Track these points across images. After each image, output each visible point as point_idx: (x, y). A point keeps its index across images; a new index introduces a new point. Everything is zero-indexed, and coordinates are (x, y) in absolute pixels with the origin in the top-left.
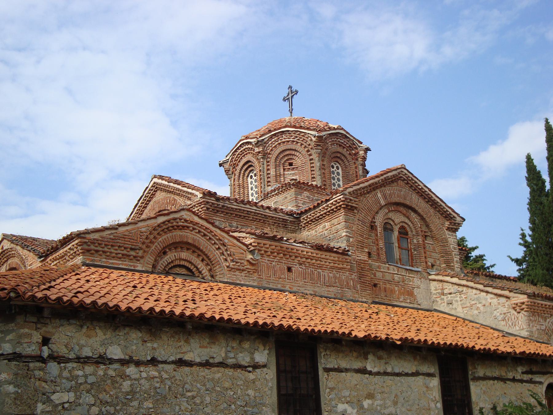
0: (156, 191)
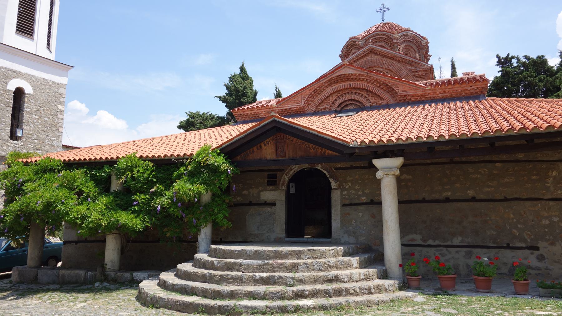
0: (370, 53)
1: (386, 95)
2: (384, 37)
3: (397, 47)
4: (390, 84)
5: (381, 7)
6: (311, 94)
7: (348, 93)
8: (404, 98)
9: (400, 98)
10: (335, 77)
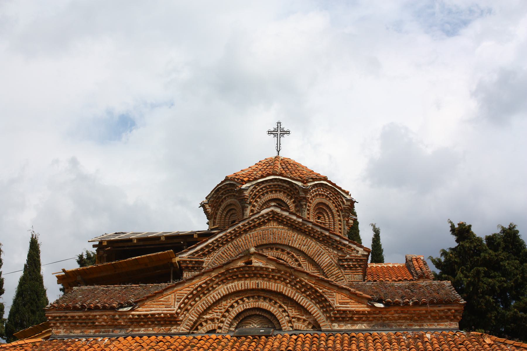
1: (315, 307)
2: (285, 185)
3: (306, 205)
4: (321, 291)
6: (192, 293)
7: (253, 297)
8: (341, 314)
9: (336, 314)
10: (233, 269)
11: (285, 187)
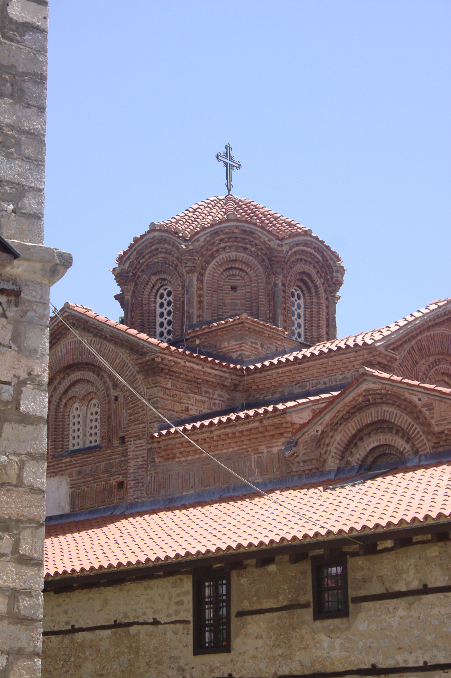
2: (318, 256)
5: (225, 151)
11: (318, 258)
